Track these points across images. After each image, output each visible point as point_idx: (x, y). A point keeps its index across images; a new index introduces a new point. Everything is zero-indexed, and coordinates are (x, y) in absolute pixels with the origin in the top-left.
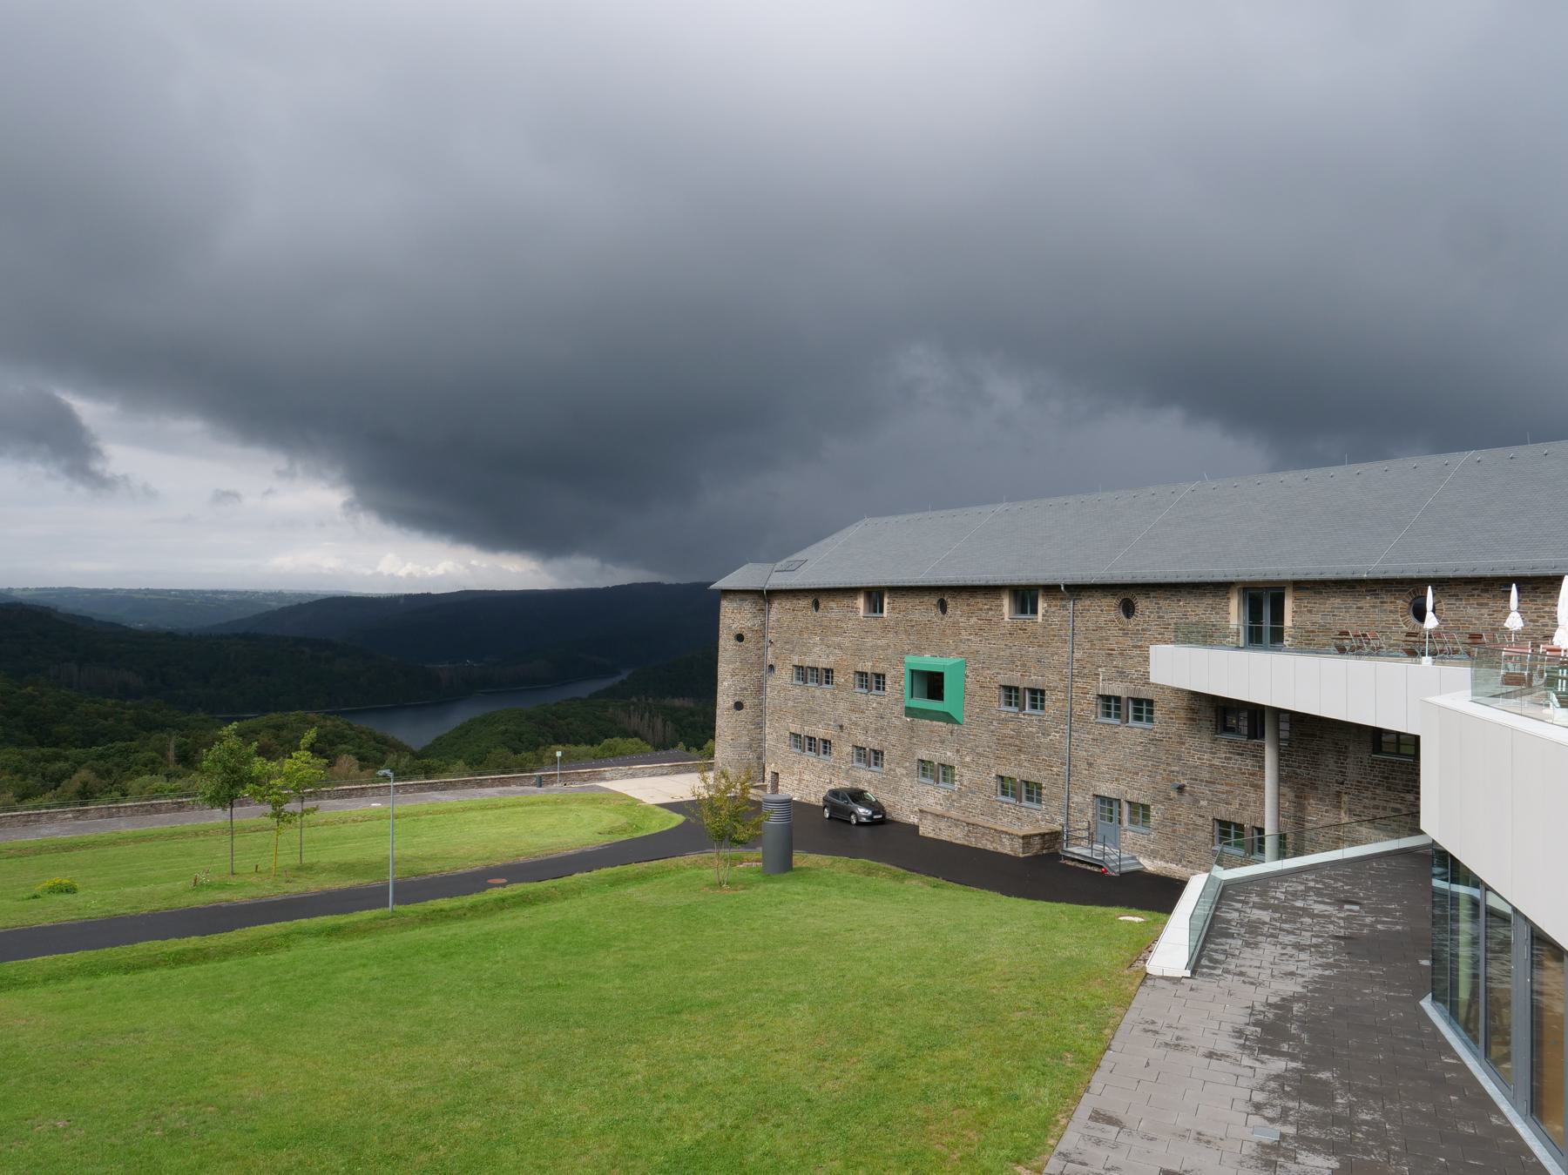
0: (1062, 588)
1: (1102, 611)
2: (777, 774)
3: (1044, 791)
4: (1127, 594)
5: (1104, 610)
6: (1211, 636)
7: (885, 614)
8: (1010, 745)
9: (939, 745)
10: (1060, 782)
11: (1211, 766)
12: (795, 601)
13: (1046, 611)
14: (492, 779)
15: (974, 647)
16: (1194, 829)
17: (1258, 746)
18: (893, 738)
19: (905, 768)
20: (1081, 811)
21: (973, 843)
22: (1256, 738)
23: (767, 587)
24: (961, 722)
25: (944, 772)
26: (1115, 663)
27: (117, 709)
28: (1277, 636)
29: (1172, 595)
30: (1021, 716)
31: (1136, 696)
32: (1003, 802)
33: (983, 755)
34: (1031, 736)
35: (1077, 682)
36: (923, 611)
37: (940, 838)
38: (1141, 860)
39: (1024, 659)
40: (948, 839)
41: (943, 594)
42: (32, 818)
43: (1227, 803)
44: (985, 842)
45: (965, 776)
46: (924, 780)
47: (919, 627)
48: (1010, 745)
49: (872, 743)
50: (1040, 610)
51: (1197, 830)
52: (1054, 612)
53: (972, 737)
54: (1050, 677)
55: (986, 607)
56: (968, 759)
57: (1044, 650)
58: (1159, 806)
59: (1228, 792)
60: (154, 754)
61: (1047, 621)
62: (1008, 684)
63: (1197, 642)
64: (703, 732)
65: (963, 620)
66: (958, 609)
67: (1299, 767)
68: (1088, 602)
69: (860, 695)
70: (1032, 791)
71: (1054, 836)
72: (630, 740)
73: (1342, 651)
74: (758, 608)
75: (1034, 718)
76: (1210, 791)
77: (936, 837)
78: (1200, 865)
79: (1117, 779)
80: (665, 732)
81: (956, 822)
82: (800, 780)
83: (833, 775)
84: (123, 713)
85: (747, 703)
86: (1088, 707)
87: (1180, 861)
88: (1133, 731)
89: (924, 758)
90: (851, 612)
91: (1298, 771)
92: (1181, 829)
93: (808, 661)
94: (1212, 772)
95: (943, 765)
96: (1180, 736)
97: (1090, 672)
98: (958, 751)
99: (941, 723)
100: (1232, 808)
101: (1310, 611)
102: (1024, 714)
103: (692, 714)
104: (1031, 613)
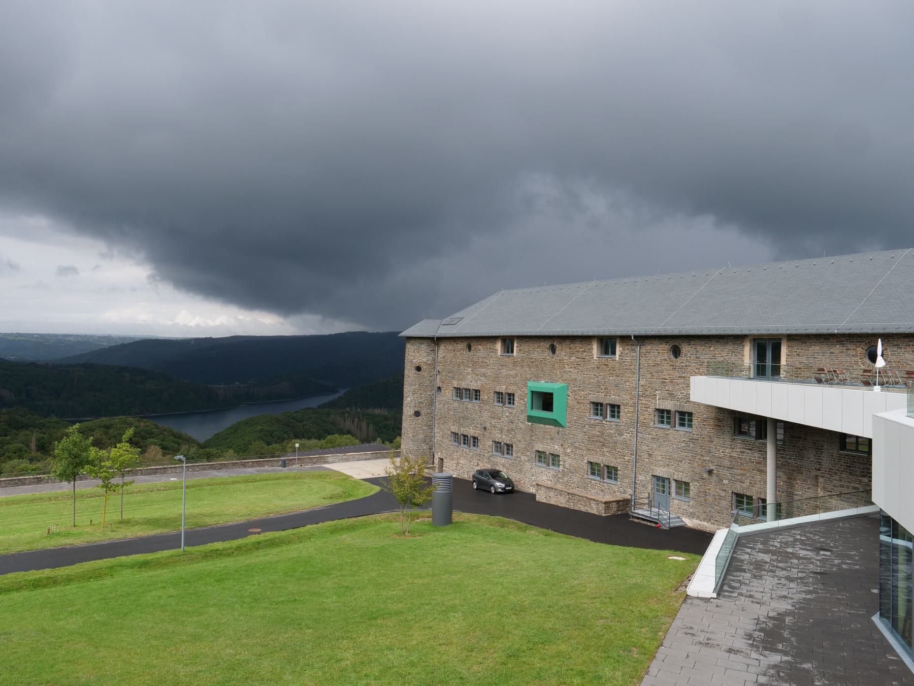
0: (633, 338)
1: (659, 353)
3: (619, 472)
5: (661, 352)
6: (731, 371)
7: (515, 354)
8: (597, 441)
9: (549, 441)
10: (630, 467)
11: (730, 457)
12: (455, 345)
13: (622, 353)
14: (252, 462)
15: (574, 376)
16: (719, 499)
17: (762, 444)
18: (519, 437)
20: (643, 486)
21: (572, 506)
22: (761, 439)
23: (437, 335)
26: (667, 388)
28: (776, 371)
29: (705, 343)
30: (604, 422)
32: (592, 480)
34: (610, 435)
35: (642, 400)
36: (540, 352)
37: (550, 503)
38: (684, 519)
39: (606, 384)
41: (553, 341)
43: (741, 482)
44: (580, 506)
45: (567, 461)
46: (540, 464)
48: (597, 441)
49: (505, 439)
50: (618, 353)
51: (722, 499)
52: (627, 354)
53: (571, 436)
55: (582, 350)
56: (569, 450)
58: (696, 483)
59: (742, 474)
61: (622, 359)
63: (722, 375)
65: (566, 358)
66: (563, 351)
67: (790, 459)
68: (649, 347)
69: (498, 407)
70: (611, 472)
71: (626, 503)
72: (345, 436)
74: (430, 349)
75: (612, 423)
76: (730, 473)
77: (547, 502)
78: (723, 523)
79: (668, 465)
80: (368, 431)
81: (561, 492)
82: (458, 464)
83: (479, 460)
85: (423, 412)
86: (650, 417)
87: (710, 520)
88: (679, 433)
89: (540, 450)
90: (492, 352)
91: (789, 461)
92: (710, 499)
93: (463, 385)
95: (552, 454)
96: (710, 437)
97: (650, 393)
98: (562, 445)
99: (551, 427)
100: (745, 485)
101: (798, 355)
102: (606, 421)
103: (386, 419)
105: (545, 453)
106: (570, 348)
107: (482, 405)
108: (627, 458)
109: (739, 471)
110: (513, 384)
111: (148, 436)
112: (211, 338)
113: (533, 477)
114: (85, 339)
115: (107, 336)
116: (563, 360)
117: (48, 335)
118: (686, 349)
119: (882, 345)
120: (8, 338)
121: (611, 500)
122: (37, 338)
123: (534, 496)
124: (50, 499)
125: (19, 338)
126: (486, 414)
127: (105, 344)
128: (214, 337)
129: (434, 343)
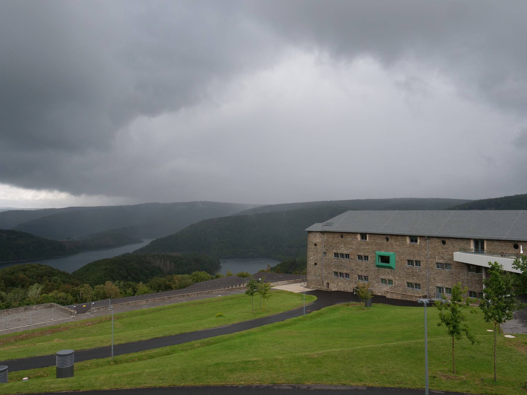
2: (328, 283)
4: (444, 240)
5: (438, 243)
7: (367, 240)
8: (410, 275)
9: (387, 274)
10: (426, 284)
11: (467, 279)
13: (420, 242)
15: (398, 250)
19: (376, 281)
20: (432, 290)
21: (404, 299)
23: (324, 230)
24: (394, 268)
25: (390, 282)
34: (416, 272)
41: (387, 237)
42: (137, 303)
46: (382, 284)
47: (379, 244)
48: (410, 275)
54: (422, 258)
56: (397, 278)
57: (420, 251)
61: (420, 244)
63: (462, 251)
66: (392, 241)
68: (432, 240)
70: (418, 286)
72: (202, 272)
73: (502, 256)
77: (392, 298)
79: (442, 283)
81: (398, 294)
82: (337, 285)
85: (318, 263)
89: (383, 278)
93: (339, 252)
94: (467, 280)
95: (388, 280)
96: (459, 272)
98: (394, 276)
100: (473, 288)
104: (415, 242)
105: (385, 279)
106: (395, 239)
107: (350, 260)
109: (471, 284)
110: (367, 252)
111: (51, 275)
113: (379, 289)
116: (393, 243)
118: (447, 241)
119: (522, 247)
123: (385, 297)
129: (322, 233)
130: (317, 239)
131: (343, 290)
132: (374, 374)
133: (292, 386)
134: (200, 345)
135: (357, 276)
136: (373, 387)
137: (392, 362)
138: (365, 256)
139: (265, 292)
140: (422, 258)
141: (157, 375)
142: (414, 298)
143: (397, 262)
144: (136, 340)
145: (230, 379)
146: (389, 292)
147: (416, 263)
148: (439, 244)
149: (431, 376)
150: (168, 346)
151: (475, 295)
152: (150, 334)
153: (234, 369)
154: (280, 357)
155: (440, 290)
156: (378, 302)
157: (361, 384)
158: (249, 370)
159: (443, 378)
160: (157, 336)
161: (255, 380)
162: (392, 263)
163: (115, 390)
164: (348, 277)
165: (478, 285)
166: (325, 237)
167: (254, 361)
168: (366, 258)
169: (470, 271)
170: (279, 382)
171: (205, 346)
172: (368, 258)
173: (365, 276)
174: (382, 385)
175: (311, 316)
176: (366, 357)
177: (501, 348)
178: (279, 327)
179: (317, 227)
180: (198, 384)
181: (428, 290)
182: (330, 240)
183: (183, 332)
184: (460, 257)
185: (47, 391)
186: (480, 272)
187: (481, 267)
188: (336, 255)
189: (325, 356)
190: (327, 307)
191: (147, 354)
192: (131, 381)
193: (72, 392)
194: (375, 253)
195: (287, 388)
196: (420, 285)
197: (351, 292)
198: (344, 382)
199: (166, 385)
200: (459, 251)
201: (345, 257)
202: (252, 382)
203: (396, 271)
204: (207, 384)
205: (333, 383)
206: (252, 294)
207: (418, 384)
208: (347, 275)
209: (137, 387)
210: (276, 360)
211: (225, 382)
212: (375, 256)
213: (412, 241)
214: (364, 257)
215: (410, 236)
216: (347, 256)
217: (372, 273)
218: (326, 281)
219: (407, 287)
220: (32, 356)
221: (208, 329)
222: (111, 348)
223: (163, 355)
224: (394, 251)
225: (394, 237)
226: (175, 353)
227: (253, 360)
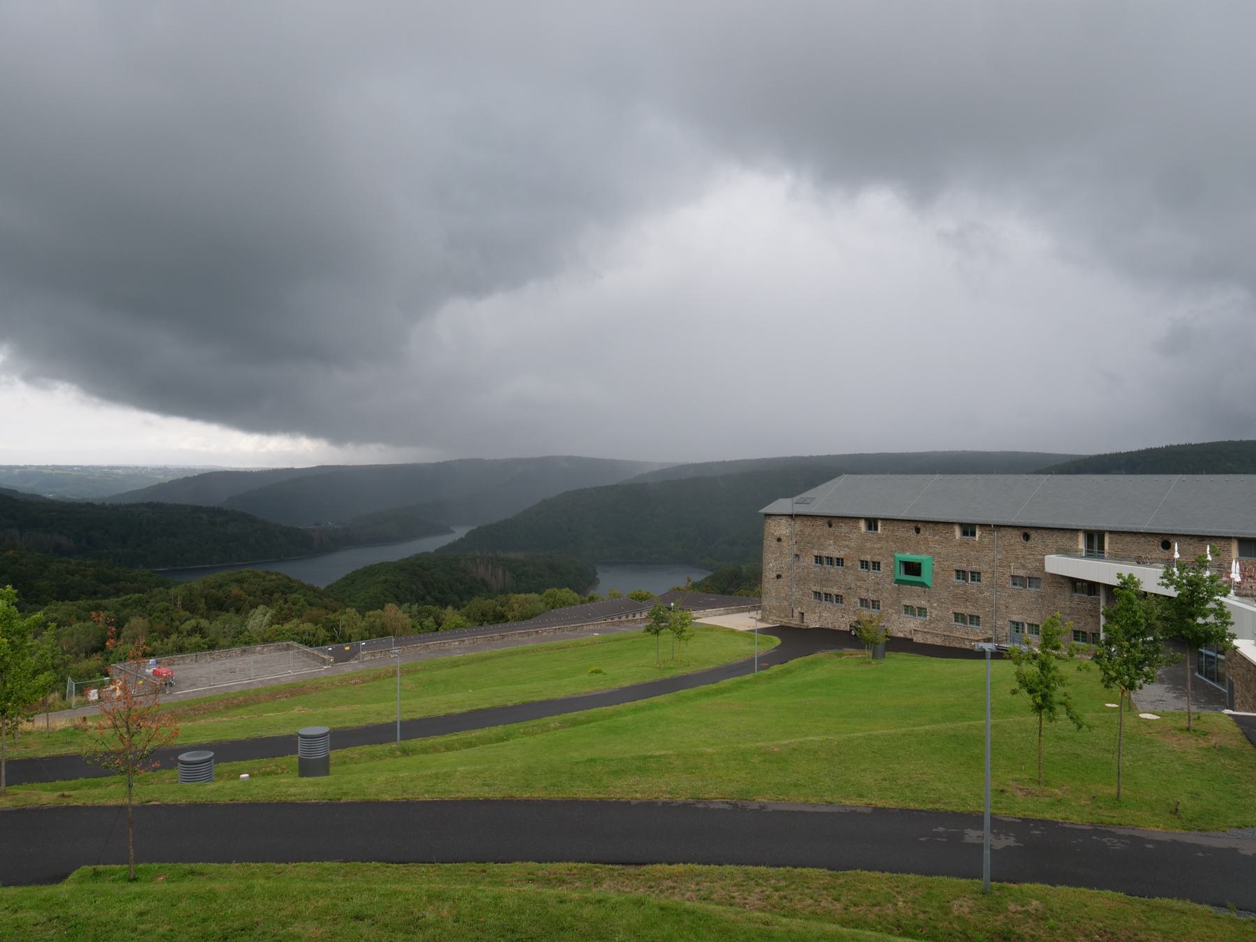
2: (803, 614)
3: (981, 620)
4: (1027, 532)
5: (1015, 538)
7: (879, 531)
10: (990, 615)
20: (1002, 628)
21: (947, 644)
23: (795, 512)
25: (922, 611)
27: (80, 567)
31: (1031, 576)
33: (942, 603)
40: (932, 643)
41: (918, 525)
42: (442, 645)
44: (954, 644)
46: (906, 615)
49: (872, 596)
56: (935, 605)
57: (979, 553)
60: (165, 603)
62: (958, 569)
63: (1062, 553)
64: (533, 579)
65: (930, 537)
66: (926, 533)
68: (1004, 533)
70: (974, 619)
72: (563, 590)
73: (1139, 563)
81: (937, 635)
82: (820, 617)
84: (86, 570)
85: (783, 575)
93: (825, 553)
95: (918, 608)
98: (929, 601)
100: (1081, 625)
101: (1116, 543)
104: (971, 535)
105: (912, 607)
108: (987, 609)
110: (879, 554)
112: (292, 469)
113: (901, 626)
114: (136, 471)
115: (162, 467)
116: (927, 538)
117: (92, 467)
118: (1033, 534)
120: (44, 471)
121: (980, 638)
122: (78, 471)
123: (912, 640)
124: (533, 651)
125: (56, 471)
126: (850, 578)
127: (161, 477)
128: (297, 466)
130: (781, 528)
131: (830, 626)
132: (886, 784)
133: (731, 804)
134: (558, 725)
135: (859, 601)
136: (884, 808)
137: (922, 761)
138: (874, 563)
139: (682, 628)
140: (985, 567)
141: (479, 777)
142: (967, 643)
143: (936, 574)
144: (442, 713)
145: (615, 787)
146: (918, 631)
147: (972, 576)
148: (1018, 540)
149: (996, 790)
150: (500, 726)
151: (1086, 637)
152: (467, 703)
153: (623, 770)
154: (709, 750)
155: (1017, 628)
156: (897, 650)
157: (860, 803)
158: (652, 773)
159: (1019, 793)
160: (479, 707)
161: (661, 791)
162: (926, 576)
163: (403, 802)
164: (841, 603)
165: (1090, 620)
166: (798, 525)
167: (660, 756)
168: (876, 565)
169: (1075, 591)
170: (707, 796)
171: (569, 727)
172: (879, 566)
173: (873, 601)
174: (902, 805)
175: (770, 675)
176: (873, 752)
177: (1131, 739)
178: (707, 694)
179: (783, 505)
180: (555, 795)
181: (994, 628)
182: (807, 531)
183: (528, 699)
184: (1057, 564)
185: (283, 799)
186: (1095, 594)
187: (1098, 584)
188: (819, 559)
189: (794, 749)
190: (800, 659)
191: (461, 739)
192: (433, 786)
193: (327, 803)
194: (894, 556)
195: (721, 806)
196: (978, 617)
197: (846, 632)
198: (829, 799)
199: (498, 796)
200: (1056, 553)
201: (836, 563)
202: (656, 795)
203: (933, 591)
204: (571, 796)
205: (809, 799)
206: (657, 632)
207: (971, 804)
208: (839, 598)
209: (443, 797)
210: (701, 755)
211: (605, 794)
212: (894, 562)
213: (965, 533)
214: (871, 564)
215: (961, 525)
216: (840, 561)
217: (886, 595)
218: (799, 608)
219: (953, 623)
220: (255, 736)
221: (575, 696)
222: (396, 726)
223: (490, 741)
224: (931, 553)
225: (931, 525)
226: (513, 739)
227: (658, 754)
